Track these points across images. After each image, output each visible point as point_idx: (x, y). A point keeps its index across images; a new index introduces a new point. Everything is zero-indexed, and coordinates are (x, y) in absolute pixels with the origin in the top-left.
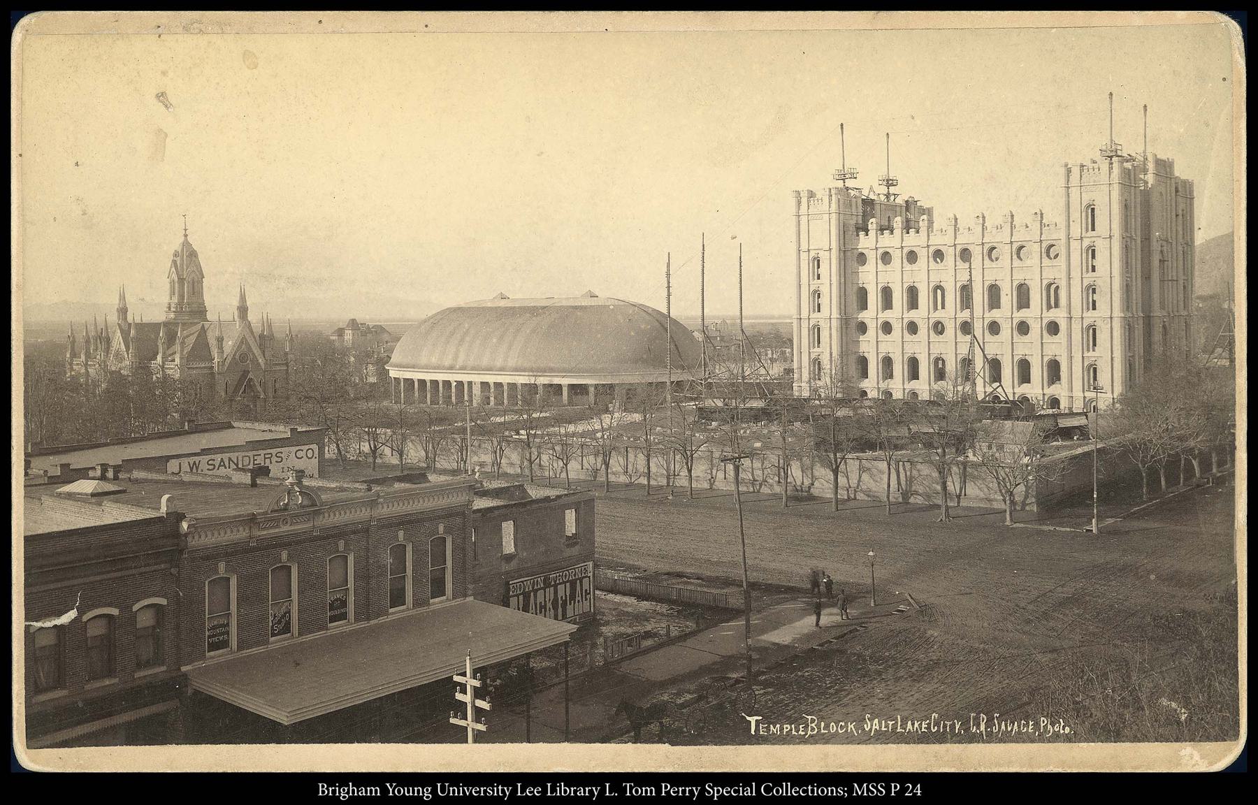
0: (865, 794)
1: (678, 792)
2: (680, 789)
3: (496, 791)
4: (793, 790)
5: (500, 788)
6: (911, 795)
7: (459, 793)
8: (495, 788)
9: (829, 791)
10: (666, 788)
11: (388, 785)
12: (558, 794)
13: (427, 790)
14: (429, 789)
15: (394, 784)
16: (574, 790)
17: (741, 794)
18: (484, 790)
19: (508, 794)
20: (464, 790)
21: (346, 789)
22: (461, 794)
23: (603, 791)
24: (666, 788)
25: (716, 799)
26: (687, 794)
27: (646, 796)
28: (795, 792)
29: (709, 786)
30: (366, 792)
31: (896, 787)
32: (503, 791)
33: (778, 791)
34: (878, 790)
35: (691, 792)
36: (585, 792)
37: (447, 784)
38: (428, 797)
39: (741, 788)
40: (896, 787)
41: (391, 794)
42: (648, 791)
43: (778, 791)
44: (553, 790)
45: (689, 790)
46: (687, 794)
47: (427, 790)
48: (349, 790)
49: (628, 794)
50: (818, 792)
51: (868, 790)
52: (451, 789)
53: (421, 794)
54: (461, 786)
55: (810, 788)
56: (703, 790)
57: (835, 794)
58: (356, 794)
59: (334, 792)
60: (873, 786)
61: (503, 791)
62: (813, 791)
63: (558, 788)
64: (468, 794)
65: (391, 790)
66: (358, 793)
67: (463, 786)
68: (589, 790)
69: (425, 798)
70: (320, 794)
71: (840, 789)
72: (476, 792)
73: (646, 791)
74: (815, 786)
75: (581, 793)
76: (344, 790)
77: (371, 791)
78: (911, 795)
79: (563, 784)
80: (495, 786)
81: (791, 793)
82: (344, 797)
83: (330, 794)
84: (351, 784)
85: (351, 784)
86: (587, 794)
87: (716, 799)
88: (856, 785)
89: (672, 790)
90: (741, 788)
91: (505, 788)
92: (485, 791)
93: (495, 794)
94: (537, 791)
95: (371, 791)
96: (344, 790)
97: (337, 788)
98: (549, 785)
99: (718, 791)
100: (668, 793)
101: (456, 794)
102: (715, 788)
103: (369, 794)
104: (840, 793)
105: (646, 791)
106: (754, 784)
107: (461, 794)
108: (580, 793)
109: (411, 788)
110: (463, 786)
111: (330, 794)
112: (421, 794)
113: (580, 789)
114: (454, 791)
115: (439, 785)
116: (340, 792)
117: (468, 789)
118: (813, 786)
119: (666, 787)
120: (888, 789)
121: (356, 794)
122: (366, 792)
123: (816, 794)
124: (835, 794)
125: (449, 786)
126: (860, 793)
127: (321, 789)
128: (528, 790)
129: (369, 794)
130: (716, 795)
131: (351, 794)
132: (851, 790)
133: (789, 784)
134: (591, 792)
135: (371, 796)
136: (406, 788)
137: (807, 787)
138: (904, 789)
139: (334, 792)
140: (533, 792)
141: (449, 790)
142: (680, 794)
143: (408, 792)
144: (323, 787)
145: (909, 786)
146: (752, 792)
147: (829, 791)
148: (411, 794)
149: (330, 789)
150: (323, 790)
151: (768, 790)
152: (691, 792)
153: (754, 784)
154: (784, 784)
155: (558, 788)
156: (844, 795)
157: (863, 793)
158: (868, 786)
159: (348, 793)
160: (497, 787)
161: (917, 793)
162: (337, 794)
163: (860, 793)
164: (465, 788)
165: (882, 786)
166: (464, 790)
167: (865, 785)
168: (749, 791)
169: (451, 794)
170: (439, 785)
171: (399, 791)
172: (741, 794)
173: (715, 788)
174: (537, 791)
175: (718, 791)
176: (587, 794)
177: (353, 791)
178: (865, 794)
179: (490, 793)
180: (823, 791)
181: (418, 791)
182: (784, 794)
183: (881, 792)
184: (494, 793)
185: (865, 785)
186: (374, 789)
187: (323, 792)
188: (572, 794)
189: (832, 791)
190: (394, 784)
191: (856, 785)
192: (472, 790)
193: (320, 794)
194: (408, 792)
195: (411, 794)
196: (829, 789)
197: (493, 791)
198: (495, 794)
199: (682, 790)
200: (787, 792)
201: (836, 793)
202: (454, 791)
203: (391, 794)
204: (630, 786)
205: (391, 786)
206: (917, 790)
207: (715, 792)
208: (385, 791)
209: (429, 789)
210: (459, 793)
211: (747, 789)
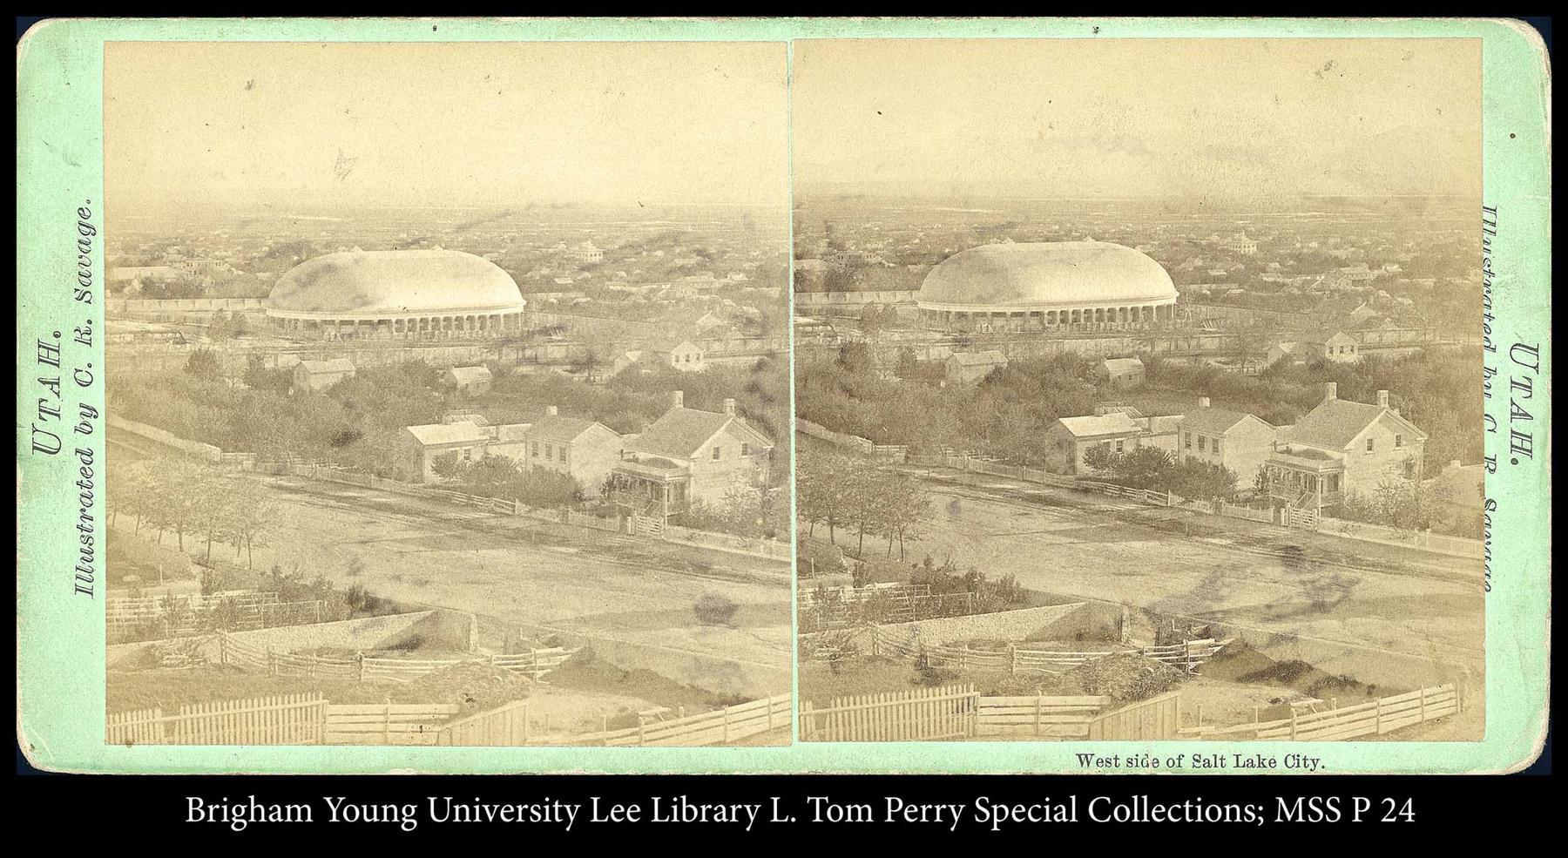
0: (1300, 819)
1: (919, 814)
2: (924, 808)
4: (1154, 811)
5: (556, 806)
7: (472, 816)
8: (547, 807)
10: (894, 806)
11: (328, 799)
12: (675, 820)
13: (408, 811)
14: (413, 808)
15: (341, 799)
16: (708, 810)
17: (1048, 819)
18: (524, 810)
19: (572, 818)
20: (482, 811)
21: (243, 808)
22: (477, 819)
23: (766, 812)
24: (894, 806)
26: (938, 819)
27: (854, 824)
28: (1158, 815)
29: (982, 803)
30: (284, 815)
32: (563, 812)
33: (1122, 813)
35: (946, 814)
36: (729, 815)
37: (448, 799)
38: (409, 825)
39: (1047, 807)
41: (334, 819)
42: (859, 813)
43: (1122, 813)
45: (942, 810)
46: (938, 819)
47: (408, 811)
48: (248, 810)
49: (818, 819)
50: (1204, 815)
53: (396, 819)
54: (477, 803)
55: (1187, 806)
58: (263, 820)
59: (218, 814)
61: (563, 812)
62: (1193, 813)
63: (675, 807)
64: (491, 819)
65: (334, 810)
66: (267, 817)
67: (480, 803)
68: (738, 810)
70: (191, 819)
73: (854, 811)
76: (239, 811)
77: (294, 811)
79: (684, 797)
80: (546, 803)
81: (1149, 816)
82: (239, 825)
83: (211, 820)
84: (252, 797)
85: (252, 797)
86: (734, 820)
89: (906, 811)
90: (1047, 807)
91: (568, 807)
92: (526, 813)
93: (547, 819)
94: (631, 813)
95: (294, 811)
96: (239, 811)
97: (225, 807)
99: (1001, 812)
100: (898, 816)
101: (467, 819)
103: (289, 820)
105: (854, 811)
107: (477, 819)
108: (720, 817)
109: (375, 807)
111: (211, 820)
112: (396, 820)
113: (720, 809)
114: (462, 813)
115: (432, 800)
116: (230, 815)
117: (491, 810)
118: (1194, 802)
119: (895, 805)
121: (263, 820)
122: (284, 815)
127: (191, 809)
128: (613, 811)
129: (289, 820)
130: (996, 820)
131: (252, 820)
134: (742, 814)
135: (294, 824)
136: (365, 807)
139: (218, 814)
140: (624, 814)
141: (453, 811)
142: (924, 819)
143: (370, 815)
144: (196, 803)
146: (1069, 815)
148: (375, 819)
149: (211, 808)
150: (196, 809)
151: (1102, 810)
152: (946, 814)
155: (675, 807)
157: (1296, 816)
159: (247, 816)
160: (551, 803)
162: (225, 820)
164: (486, 807)
166: (482, 811)
169: (457, 820)
170: (432, 800)
171: (351, 813)
172: (1048, 819)
174: (631, 813)
175: (1001, 812)
176: (734, 820)
177: (258, 811)
178: (1300, 819)
179: (535, 817)
180: (1214, 813)
181: (390, 812)
186: (299, 809)
187: (196, 815)
188: (704, 820)
189: (1233, 811)
190: (341, 799)
192: (499, 809)
193: (191, 819)
194: (370, 815)
195: (375, 819)
197: (543, 812)
198: (547, 820)
199: (928, 810)
200: (1141, 816)
202: (462, 811)
203: (334, 819)
205: (335, 802)
207: (993, 815)
208: (321, 812)
209: (413, 808)
210: (472, 816)
211: (1060, 809)
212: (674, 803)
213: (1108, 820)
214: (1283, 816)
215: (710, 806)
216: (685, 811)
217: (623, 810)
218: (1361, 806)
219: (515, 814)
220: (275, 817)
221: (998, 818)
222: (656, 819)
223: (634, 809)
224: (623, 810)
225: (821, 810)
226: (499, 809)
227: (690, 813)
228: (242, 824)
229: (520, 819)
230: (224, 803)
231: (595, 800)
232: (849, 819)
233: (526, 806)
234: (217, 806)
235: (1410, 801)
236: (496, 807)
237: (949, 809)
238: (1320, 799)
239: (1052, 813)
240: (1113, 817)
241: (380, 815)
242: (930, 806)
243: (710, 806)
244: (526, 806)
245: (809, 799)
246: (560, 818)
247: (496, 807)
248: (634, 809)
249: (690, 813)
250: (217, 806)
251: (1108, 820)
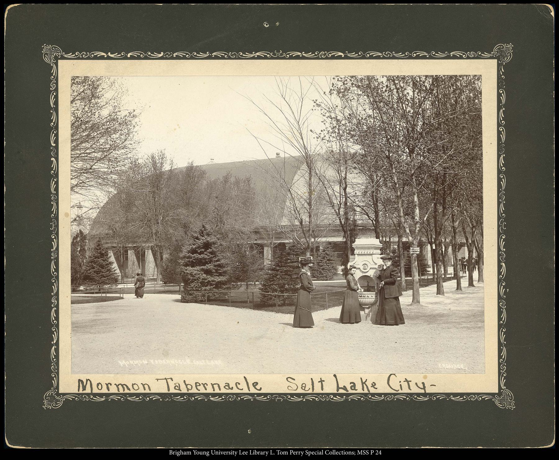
1: (296, 453)
3: (232, 453)
7: (219, 453)
9: (349, 453)
20: (220, 453)
29: (307, 451)
30: (186, 453)
31: (372, 452)
32: (234, 453)
33: (331, 453)
34: (366, 453)
35: (301, 453)
36: (263, 453)
40: (372, 452)
42: (286, 453)
43: (331, 453)
44: (252, 453)
50: (345, 453)
51: (363, 452)
56: (305, 452)
59: (175, 453)
60: (364, 451)
61: (234, 453)
62: (343, 453)
73: (285, 453)
75: (262, 454)
77: (188, 453)
82: (178, 455)
92: (228, 453)
94: (246, 453)
95: (188, 453)
100: (292, 454)
105: (285, 453)
114: (217, 453)
118: (343, 451)
119: (292, 452)
120: (370, 452)
122: (186, 453)
132: (357, 453)
134: (265, 453)
135: (188, 455)
138: (375, 452)
139: (175, 453)
144: (171, 451)
146: (322, 453)
147: (349, 453)
150: (171, 452)
151: (327, 452)
152: (301, 453)
157: (361, 453)
158: (362, 451)
159: (180, 454)
160: (232, 451)
166: (220, 453)
171: (198, 453)
174: (246, 453)
177: (182, 453)
180: (347, 453)
181: (205, 453)
183: (367, 453)
187: (171, 453)
189: (350, 453)
197: (231, 453)
202: (217, 453)
207: (309, 453)
208: (193, 453)
210: (219, 453)
219: (226, 453)
239: (319, 453)
241: (203, 453)
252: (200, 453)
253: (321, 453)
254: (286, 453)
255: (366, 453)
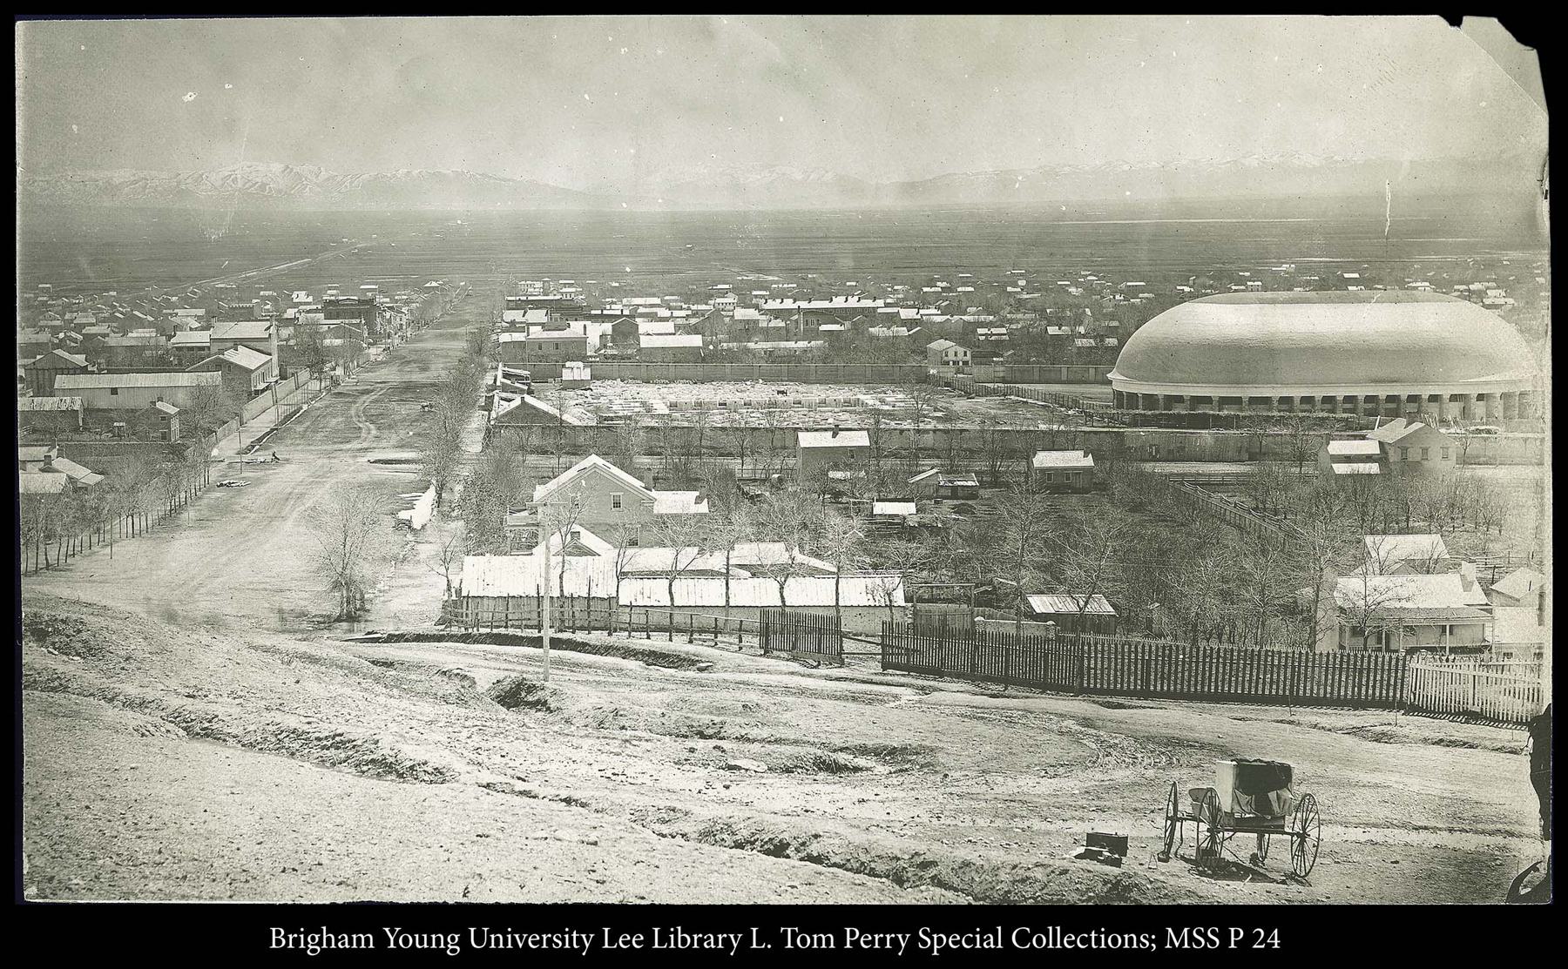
0: (1186, 946)
1: (873, 942)
2: (877, 936)
4: (1065, 939)
5: (575, 935)
6: (1263, 946)
7: (505, 943)
8: (567, 936)
9: (1126, 941)
10: (851, 935)
11: (387, 930)
12: (672, 946)
13: (453, 939)
14: (456, 936)
15: (398, 929)
17: (978, 946)
18: (548, 939)
19: (587, 945)
20: (514, 939)
21: (317, 936)
22: (510, 946)
25: (935, 953)
26: (888, 946)
27: (819, 949)
29: (925, 932)
30: (351, 943)
32: (580, 940)
33: (1039, 941)
35: (895, 942)
36: (716, 943)
37: (486, 929)
38: (453, 951)
39: (978, 936)
41: (392, 946)
42: (822, 941)
43: (1039, 941)
44: (664, 938)
45: (891, 939)
46: (888, 946)
47: (453, 939)
48: (321, 939)
49: (789, 946)
52: (493, 936)
53: (442, 946)
54: (509, 933)
55: (1093, 935)
56: (915, 939)
57: (1135, 946)
58: (333, 946)
60: (1199, 932)
61: (580, 940)
62: (1098, 941)
63: (672, 936)
64: (521, 945)
65: (392, 939)
66: (336, 944)
67: (512, 933)
68: (723, 939)
69: (448, 952)
70: (274, 946)
71: (1145, 937)
72: (533, 943)
73: (820, 939)
74: (1102, 933)
75: (710, 944)
76: (313, 939)
77: (359, 940)
78: (1263, 946)
79: (679, 928)
80: (566, 933)
81: (1062, 944)
82: (313, 951)
83: (291, 946)
84: (324, 928)
85: (324, 928)
86: (720, 946)
87: (935, 953)
88: (1170, 930)
89: (862, 939)
90: (978, 936)
91: (584, 936)
92: (550, 941)
93: (567, 946)
94: (636, 941)
95: (359, 940)
96: (313, 939)
97: (302, 936)
98: (656, 930)
99: (940, 941)
100: (856, 943)
101: (501, 946)
102: (935, 936)
103: (355, 946)
104: (1144, 944)
105: (820, 939)
106: (999, 928)
107: (510, 946)
108: (709, 944)
109: (425, 936)
110: (512, 933)
111: (291, 946)
112: (442, 946)
113: (709, 938)
114: (496, 941)
115: (472, 930)
116: (306, 943)
117: (521, 938)
119: (852, 934)
120: (1225, 938)
121: (333, 946)
122: (351, 943)
123: (1103, 946)
124: (1135, 946)
125: (489, 933)
126: (1177, 944)
127: (274, 937)
128: (621, 939)
129: (355, 946)
130: (936, 947)
131: (325, 946)
133: (1058, 928)
134: (727, 942)
135: (358, 950)
136: (417, 936)
137: (1089, 933)
138: (1251, 938)
140: (630, 942)
141: (489, 939)
142: (877, 946)
143: (421, 942)
144: (278, 933)
145: (1259, 933)
146: (996, 943)
147: (1126, 941)
148: (426, 946)
149: (291, 937)
150: (279, 938)
151: (1023, 938)
152: (895, 942)
153: (999, 928)
154: (1050, 928)
155: (672, 936)
156: (1151, 947)
157: (1182, 943)
158: (1190, 933)
159: (320, 943)
160: (570, 933)
161: (1273, 944)
162: (302, 946)
163: (1177, 944)
164: (517, 936)
165: (1213, 932)
166: (514, 939)
167: (1186, 930)
168: (992, 940)
169: (493, 946)
171: (406, 941)
172: (978, 946)
173: (935, 936)
174: (636, 941)
175: (940, 941)
176: (720, 946)
177: (329, 939)
178: (1186, 946)
179: (557, 944)
180: (1115, 941)
181: (438, 939)
182: (1051, 946)
183: (1213, 943)
184: (564, 944)
185: (1186, 930)
186: (363, 937)
187: (278, 942)
188: (696, 946)
189: (1131, 939)
190: (398, 929)
191: (1170, 930)
192: (527, 938)
193: (274, 946)
194: (421, 942)
195: (426, 946)
196: (1126, 936)
197: (563, 940)
198: (567, 946)
199: (880, 939)
200: (1055, 943)
201: (1138, 945)
202: (497, 939)
203: (392, 946)
204: (793, 932)
205: (392, 932)
206: (1273, 939)
207: (933, 942)
208: (382, 940)
209: (456, 936)
210: (505, 943)
211: (989, 938)
212: (672, 933)
213: (1028, 946)
214: (1172, 943)
215: (701, 935)
216: (680, 939)
217: (629, 938)
218: (1236, 935)
220: (343, 944)
221: (938, 945)
222: (656, 946)
223: (639, 937)
224: (629, 938)
225: (793, 939)
226: (527, 938)
227: (684, 941)
228: (316, 950)
229: (545, 946)
230: (301, 933)
231: (606, 930)
232: (815, 946)
233: (550, 935)
234: (296, 935)
235: (1276, 931)
236: (525, 936)
237: (897, 937)
238: (1202, 929)
239: (982, 941)
240: (1032, 945)
241: (430, 943)
242: (882, 935)
243: (701, 935)
244: (550, 935)
245: (782, 929)
246: (577, 945)
247: (525, 936)
248: (639, 937)
249: (684, 941)
250: (296, 935)
251: (1028, 946)
252: (415, 941)
253: (992, 942)
254: (828, 940)
255: (1205, 936)
